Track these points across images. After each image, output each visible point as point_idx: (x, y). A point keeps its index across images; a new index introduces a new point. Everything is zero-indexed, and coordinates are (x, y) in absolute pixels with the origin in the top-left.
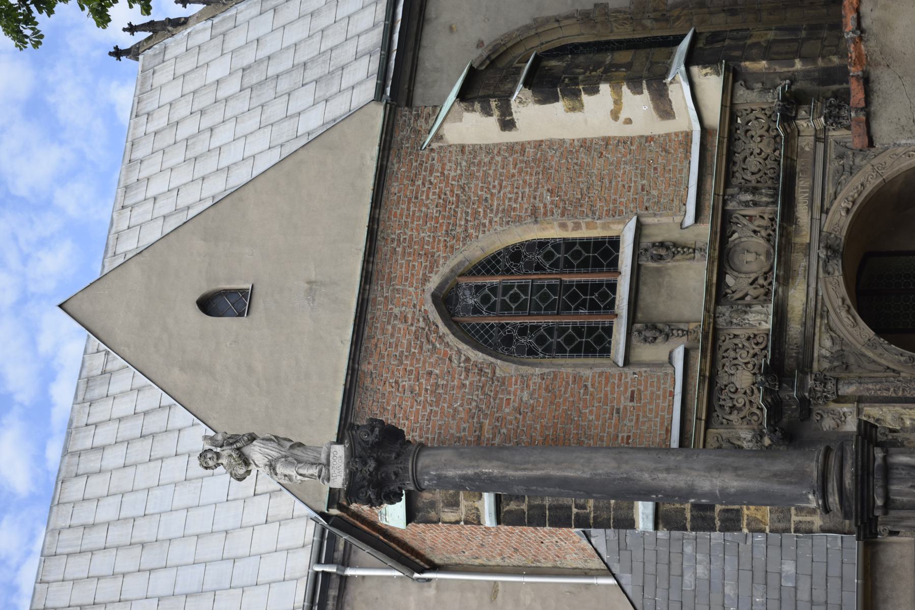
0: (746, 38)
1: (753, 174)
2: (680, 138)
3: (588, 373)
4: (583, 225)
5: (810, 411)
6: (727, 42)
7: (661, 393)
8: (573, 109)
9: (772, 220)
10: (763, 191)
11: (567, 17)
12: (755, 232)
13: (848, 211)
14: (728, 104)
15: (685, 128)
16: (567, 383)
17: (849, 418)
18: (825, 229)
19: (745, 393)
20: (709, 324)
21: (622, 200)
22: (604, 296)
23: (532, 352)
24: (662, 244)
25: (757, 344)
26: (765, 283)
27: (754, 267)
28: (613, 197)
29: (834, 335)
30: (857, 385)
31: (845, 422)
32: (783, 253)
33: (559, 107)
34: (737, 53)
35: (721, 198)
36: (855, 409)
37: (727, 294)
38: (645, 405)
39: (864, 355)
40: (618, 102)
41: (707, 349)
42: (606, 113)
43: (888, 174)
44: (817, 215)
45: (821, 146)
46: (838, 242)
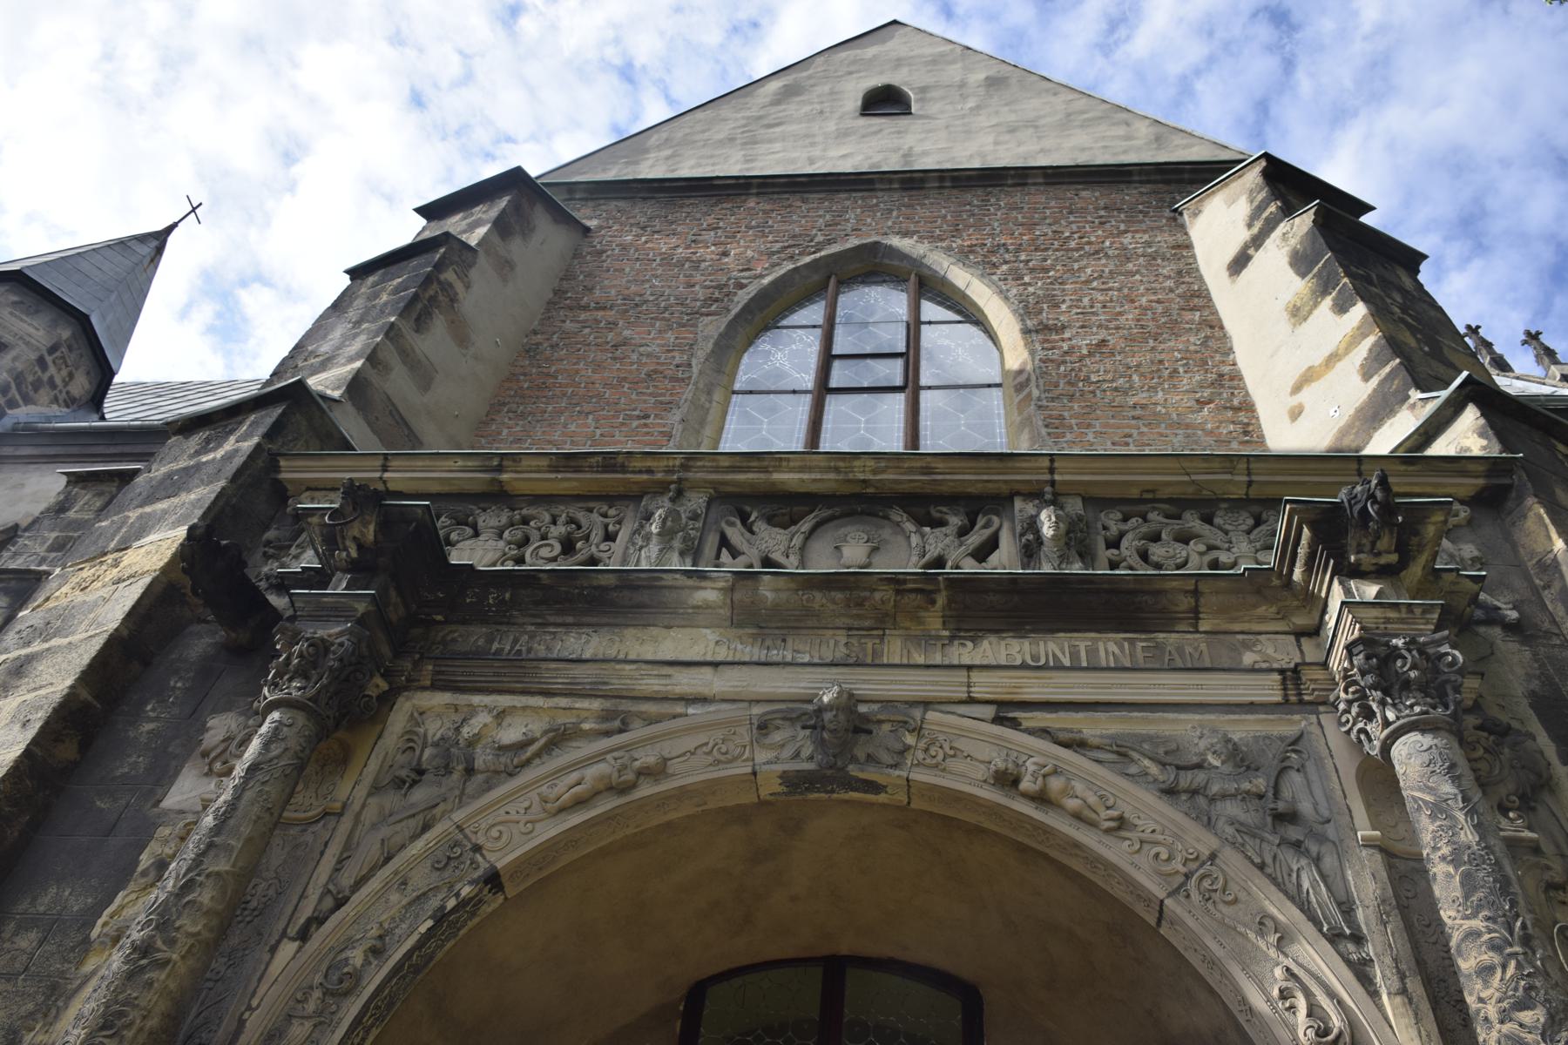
1: (1144, 556)
13: (1008, 780)
18: (931, 715)
20: (649, 471)
35: (1047, 477)
39: (426, 827)
45: (1268, 689)
46: (886, 758)
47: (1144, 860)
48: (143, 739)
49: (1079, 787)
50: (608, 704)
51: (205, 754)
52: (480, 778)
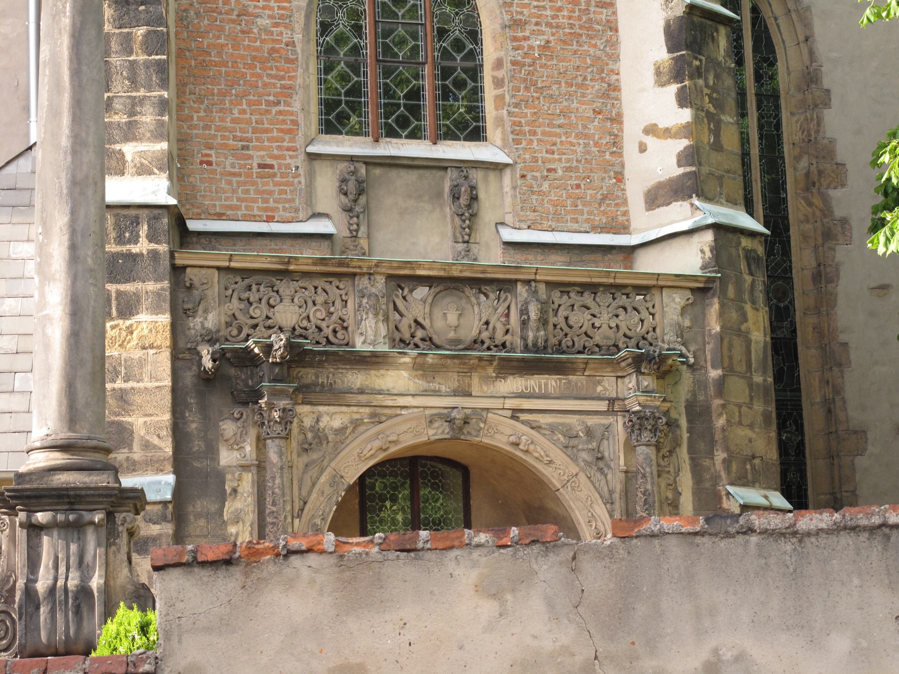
0: (753, 302)
1: (566, 318)
2: (620, 218)
3: (296, 106)
4: (499, 92)
5: (245, 404)
6: (748, 279)
7: (272, 204)
8: (658, 73)
9: (504, 345)
10: (542, 333)
11: (811, 53)
12: (487, 323)
14: (661, 283)
15: (634, 225)
16: (283, 78)
17: (236, 454)
18: (490, 415)
19: (268, 318)
20: (360, 267)
21: (535, 143)
22: (403, 122)
23: (325, 28)
24: (474, 198)
25: (335, 331)
26: (417, 340)
27: (439, 323)
28: (539, 130)
29: (348, 431)
30: (279, 464)
31: (232, 449)
32: (457, 361)
33: (661, 53)
34: (731, 292)
35: (532, 277)
36: (249, 463)
37: (402, 289)
38: (254, 184)
39: (322, 471)
40: (667, 133)
41: (326, 265)
42: (654, 116)
43: (566, 495)
44: (511, 403)
45: (603, 406)
46: (474, 433)
47: (555, 475)
48: (195, 432)
49: (539, 449)
50: (372, 409)
51: (226, 441)
52: (331, 444)
